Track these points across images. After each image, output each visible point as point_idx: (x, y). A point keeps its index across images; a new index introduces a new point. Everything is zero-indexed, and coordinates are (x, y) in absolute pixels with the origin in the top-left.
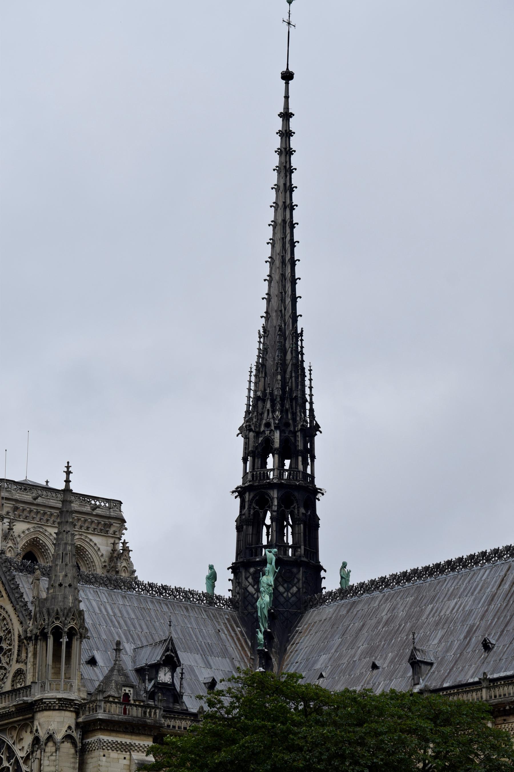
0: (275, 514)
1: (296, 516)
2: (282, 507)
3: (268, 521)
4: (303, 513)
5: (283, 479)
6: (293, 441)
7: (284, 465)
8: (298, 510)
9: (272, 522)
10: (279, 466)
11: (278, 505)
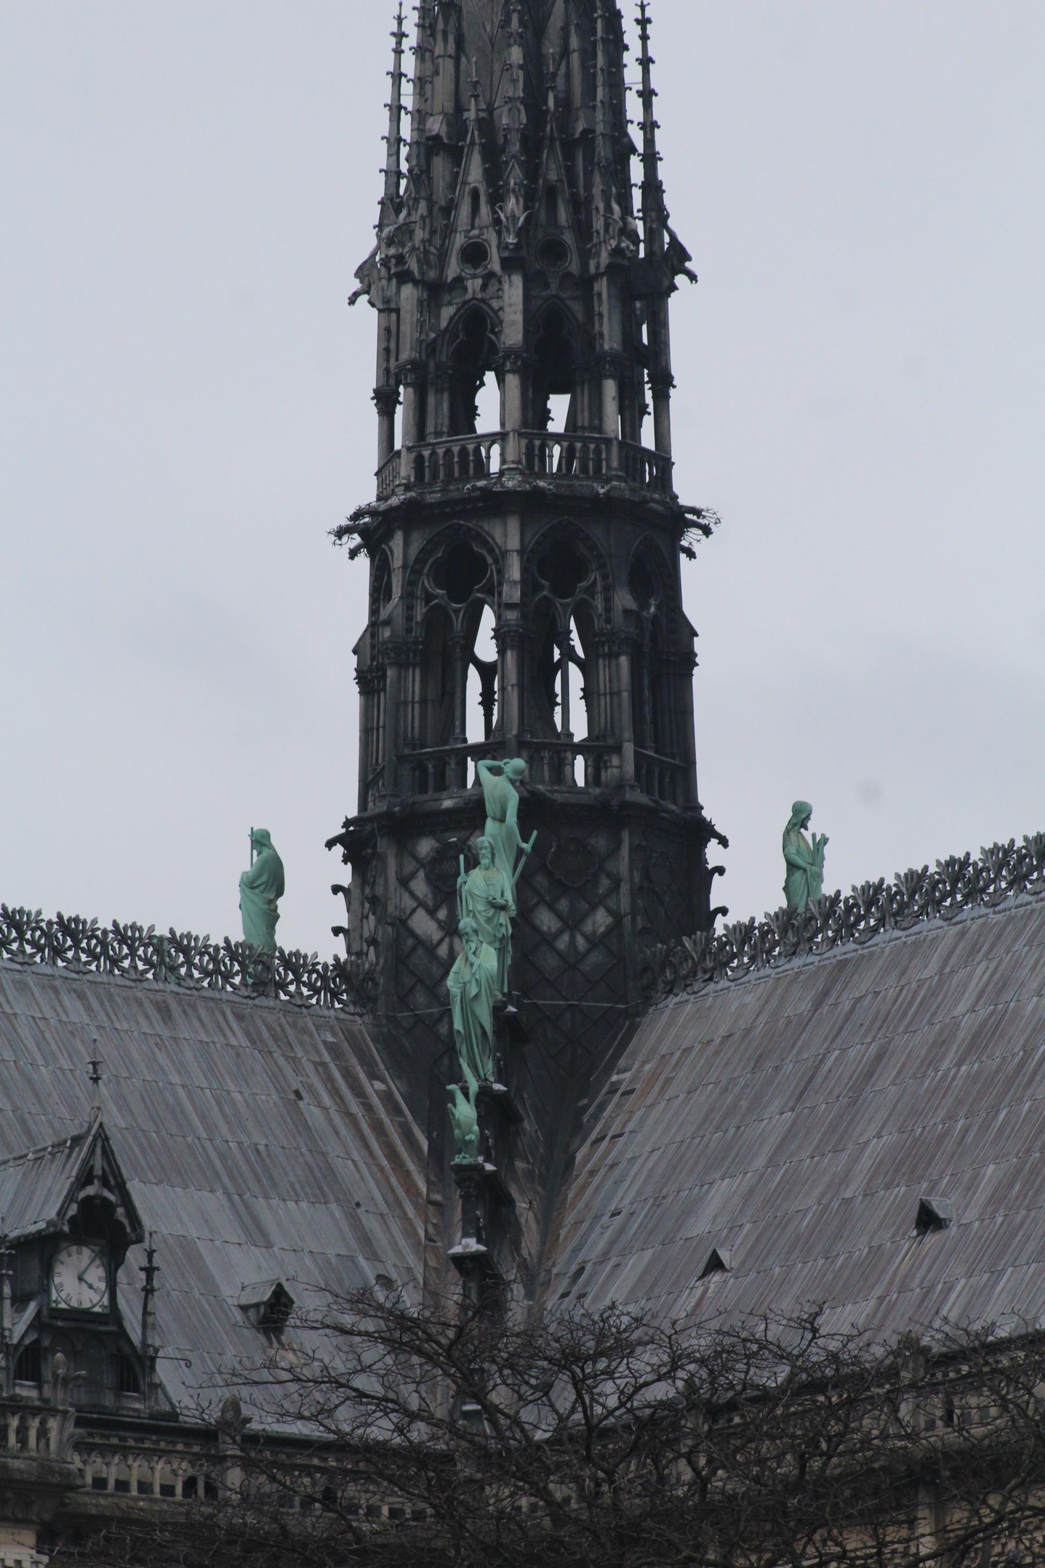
0: (512, 616)
1: (598, 624)
2: (541, 588)
3: (486, 648)
4: (627, 612)
5: (542, 474)
6: (580, 316)
7: (545, 416)
8: (608, 600)
9: (501, 652)
10: (524, 423)
11: (524, 581)
